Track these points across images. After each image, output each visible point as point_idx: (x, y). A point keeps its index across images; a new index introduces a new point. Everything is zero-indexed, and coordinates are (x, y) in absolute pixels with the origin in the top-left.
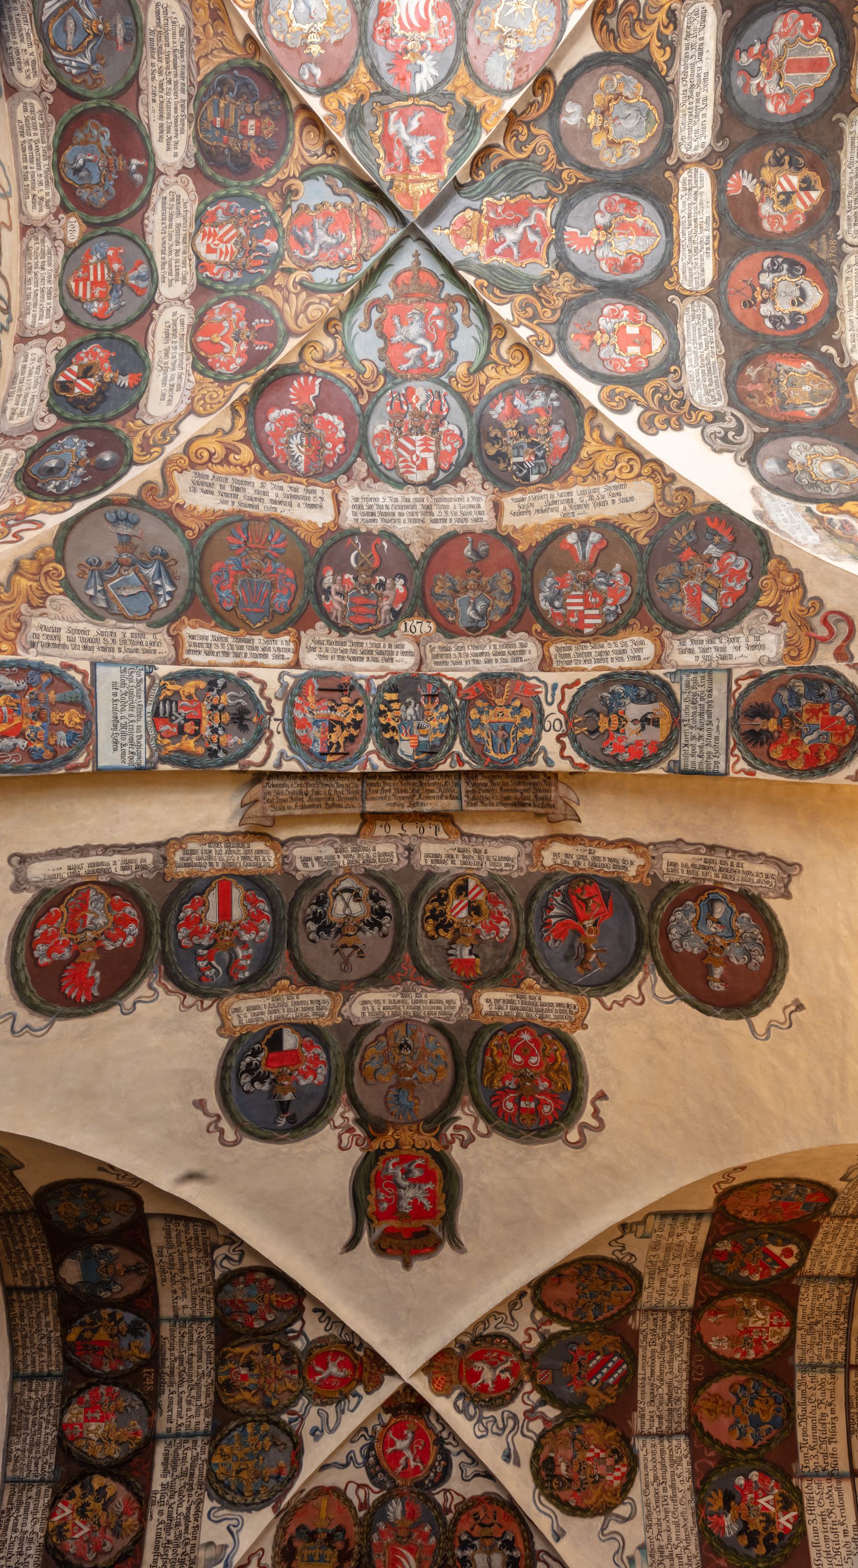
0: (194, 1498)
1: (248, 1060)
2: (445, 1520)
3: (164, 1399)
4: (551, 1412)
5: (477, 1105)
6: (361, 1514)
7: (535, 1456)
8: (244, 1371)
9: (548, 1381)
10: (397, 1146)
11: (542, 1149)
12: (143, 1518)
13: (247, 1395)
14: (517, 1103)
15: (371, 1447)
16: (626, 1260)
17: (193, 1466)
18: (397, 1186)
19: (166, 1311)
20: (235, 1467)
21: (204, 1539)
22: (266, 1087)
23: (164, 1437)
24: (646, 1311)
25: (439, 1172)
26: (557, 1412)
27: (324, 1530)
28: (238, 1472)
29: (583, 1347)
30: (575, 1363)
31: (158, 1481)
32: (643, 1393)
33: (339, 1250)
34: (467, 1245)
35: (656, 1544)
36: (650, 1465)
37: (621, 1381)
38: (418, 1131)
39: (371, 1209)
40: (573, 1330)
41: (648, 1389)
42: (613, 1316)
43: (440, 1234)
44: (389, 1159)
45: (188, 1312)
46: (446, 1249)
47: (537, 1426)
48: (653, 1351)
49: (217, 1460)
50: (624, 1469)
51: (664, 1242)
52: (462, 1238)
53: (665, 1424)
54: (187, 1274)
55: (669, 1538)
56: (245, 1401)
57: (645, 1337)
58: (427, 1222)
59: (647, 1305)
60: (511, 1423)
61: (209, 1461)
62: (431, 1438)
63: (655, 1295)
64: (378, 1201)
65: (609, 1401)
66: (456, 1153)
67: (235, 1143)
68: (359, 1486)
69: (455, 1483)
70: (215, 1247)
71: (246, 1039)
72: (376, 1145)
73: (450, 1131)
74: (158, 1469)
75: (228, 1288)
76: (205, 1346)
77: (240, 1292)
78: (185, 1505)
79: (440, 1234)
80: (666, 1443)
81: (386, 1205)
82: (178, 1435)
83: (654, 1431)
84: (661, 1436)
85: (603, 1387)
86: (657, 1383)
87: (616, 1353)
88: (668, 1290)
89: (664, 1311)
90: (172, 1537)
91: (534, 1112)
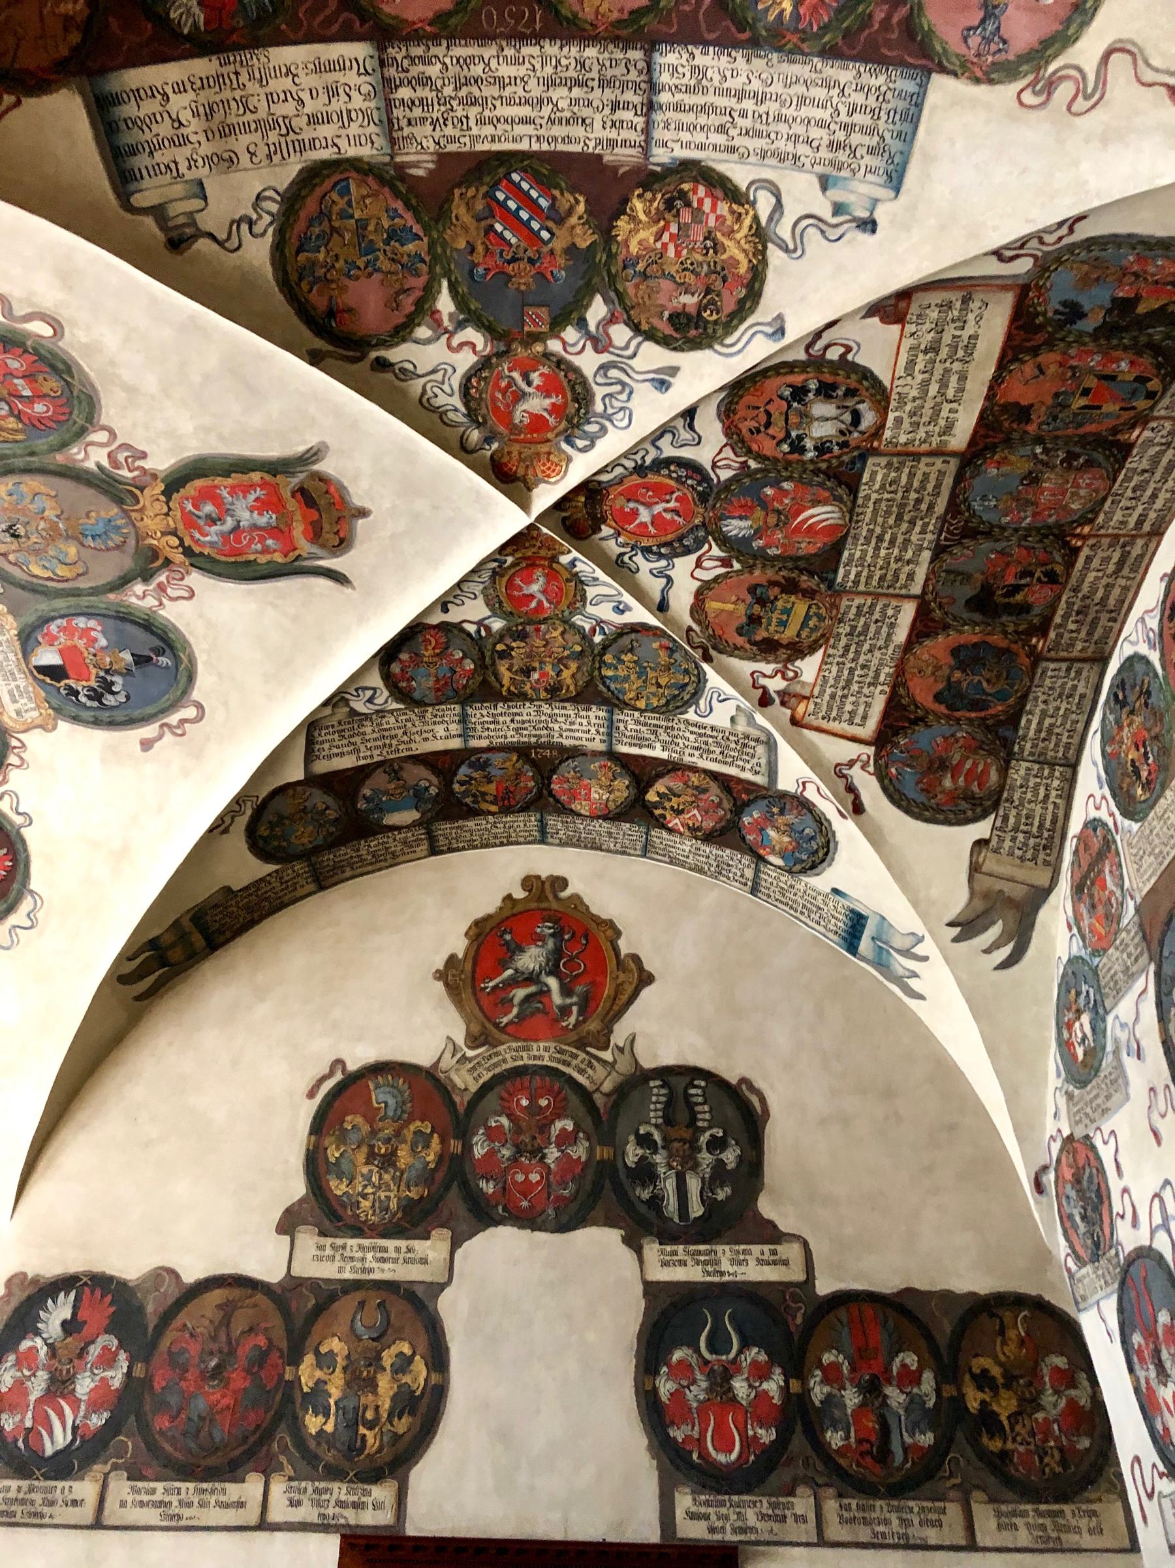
0: (682, 727)
1: (83, 699)
2: (757, 471)
3: (567, 743)
4: (597, 310)
5: (64, 445)
6: (737, 566)
7: (665, 342)
8: (535, 676)
9: (544, 312)
10: (174, 533)
11: (89, 366)
12: (694, 769)
13: (566, 674)
14: (30, 400)
15: (647, 551)
16: (274, 208)
17: (646, 724)
18: (236, 528)
19: (456, 744)
20: (653, 689)
21: (727, 724)
22: (118, 680)
23: (611, 744)
24: (393, 142)
25: (199, 483)
26: (598, 299)
27: (750, 606)
28: (659, 686)
29: (479, 256)
30: (510, 269)
31: (659, 753)
32: (568, 139)
33: (348, 591)
34: (311, 441)
35: (824, 153)
36: (700, 137)
37: (544, 183)
38: (141, 510)
39: (278, 558)
40: (447, 274)
41: (558, 131)
42: (408, 205)
43: (302, 476)
44: (197, 542)
45: (455, 728)
46: (325, 466)
47: (620, 334)
48: (480, 122)
49: (641, 704)
50: (702, 191)
51: (206, 149)
52: (301, 449)
53: (629, 96)
54: (400, 732)
55: (821, 124)
56: (573, 676)
57: (452, 140)
58: (286, 493)
59: (380, 142)
60: (613, 373)
61: (642, 711)
62: (636, 480)
63: (354, 129)
64: (266, 550)
65: (581, 208)
66: (161, 461)
67: (199, 706)
68: (699, 564)
69: (704, 455)
70: (353, 713)
71: (55, 702)
72: (178, 557)
73: (125, 473)
74: (646, 752)
75: (417, 695)
76: (499, 710)
77: (423, 684)
78: (687, 735)
79: (302, 476)
80: (664, 98)
81: (270, 542)
82: (610, 735)
83: (640, 121)
84: (650, 107)
85: (557, 217)
86: (546, 110)
87: (490, 196)
88: (338, 104)
89: (389, 104)
90: (718, 750)
91: (29, 377)
